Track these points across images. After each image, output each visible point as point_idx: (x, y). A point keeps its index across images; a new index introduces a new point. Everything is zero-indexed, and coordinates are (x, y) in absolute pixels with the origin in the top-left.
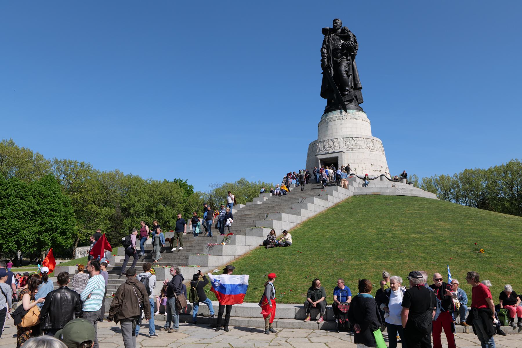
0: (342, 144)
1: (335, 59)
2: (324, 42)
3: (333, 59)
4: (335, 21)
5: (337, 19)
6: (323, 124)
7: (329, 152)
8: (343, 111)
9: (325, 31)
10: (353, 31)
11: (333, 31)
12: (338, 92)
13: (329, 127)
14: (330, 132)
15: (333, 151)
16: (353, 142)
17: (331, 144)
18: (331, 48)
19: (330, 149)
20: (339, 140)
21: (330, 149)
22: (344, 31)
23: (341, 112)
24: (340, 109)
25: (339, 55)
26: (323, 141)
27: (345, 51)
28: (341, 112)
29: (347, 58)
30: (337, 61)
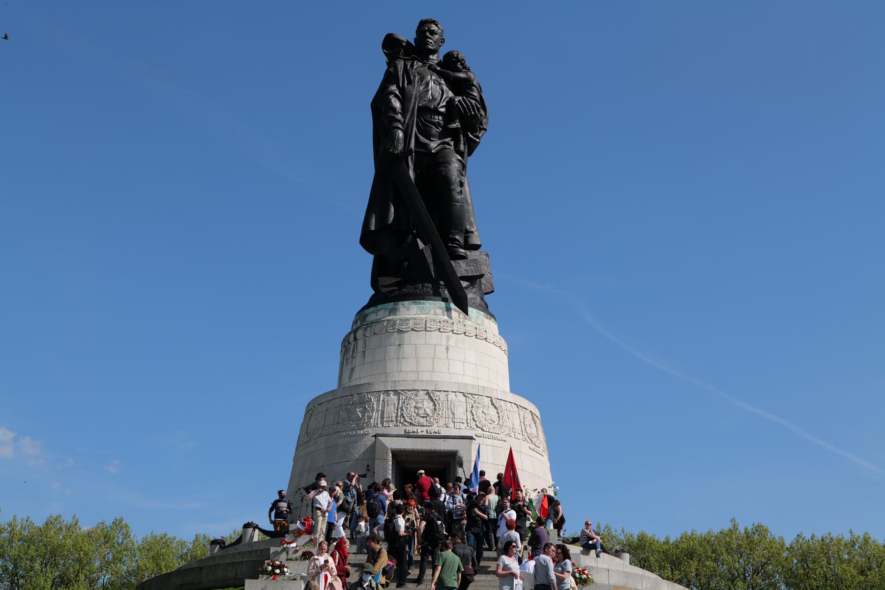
0: (460, 412)
1: (422, 138)
2: (390, 77)
3: (417, 138)
5: (434, 22)
6: (363, 335)
7: (421, 431)
8: (452, 305)
9: (391, 44)
11: (420, 49)
12: (417, 244)
13: (407, 350)
14: (408, 365)
15: (434, 429)
16: (492, 411)
17: (428, 406)
19: (422, 420)
20: (452, 396)
21: (422, 420)
22: (451, 62)
23: (448, 309)
24: (445, 300)
25: (435, 130)
26: (396, 392)
27: (456, 125)
28: (448, 309)
29: (457, 146)
30: (426, 146)
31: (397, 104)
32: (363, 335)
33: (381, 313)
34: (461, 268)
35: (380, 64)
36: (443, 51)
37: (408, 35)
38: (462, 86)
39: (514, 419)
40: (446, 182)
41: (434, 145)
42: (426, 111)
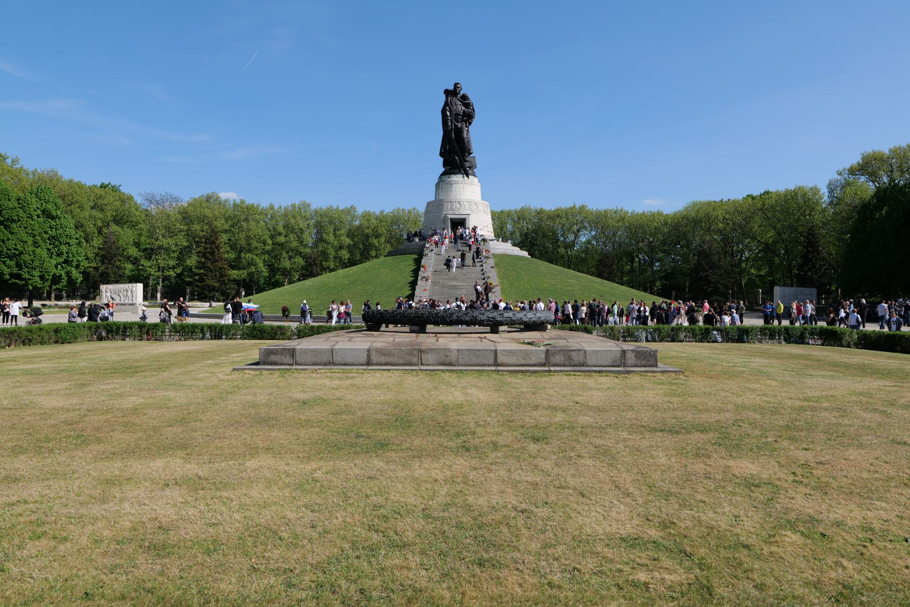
0: (467, 207)
2: (446, 104)
4: (456, 84)
10: (472, 99)
14: (453, 193)
18: (453, 113)
22: (464, 97)
31: (448, 113)
32: (441, 183)
33: (445, 178)
34: (467, 164)
35: (443, 98)
36: (462, 93)
37: (451, 88)
38: (467, 105)
39: (481, 208)
40: (463, 139)
41: (459, 125)
42: (457, 115)
